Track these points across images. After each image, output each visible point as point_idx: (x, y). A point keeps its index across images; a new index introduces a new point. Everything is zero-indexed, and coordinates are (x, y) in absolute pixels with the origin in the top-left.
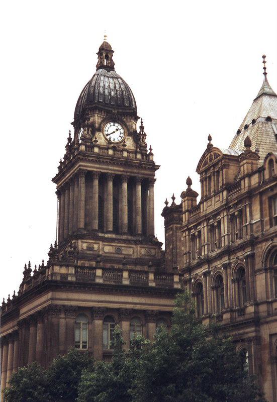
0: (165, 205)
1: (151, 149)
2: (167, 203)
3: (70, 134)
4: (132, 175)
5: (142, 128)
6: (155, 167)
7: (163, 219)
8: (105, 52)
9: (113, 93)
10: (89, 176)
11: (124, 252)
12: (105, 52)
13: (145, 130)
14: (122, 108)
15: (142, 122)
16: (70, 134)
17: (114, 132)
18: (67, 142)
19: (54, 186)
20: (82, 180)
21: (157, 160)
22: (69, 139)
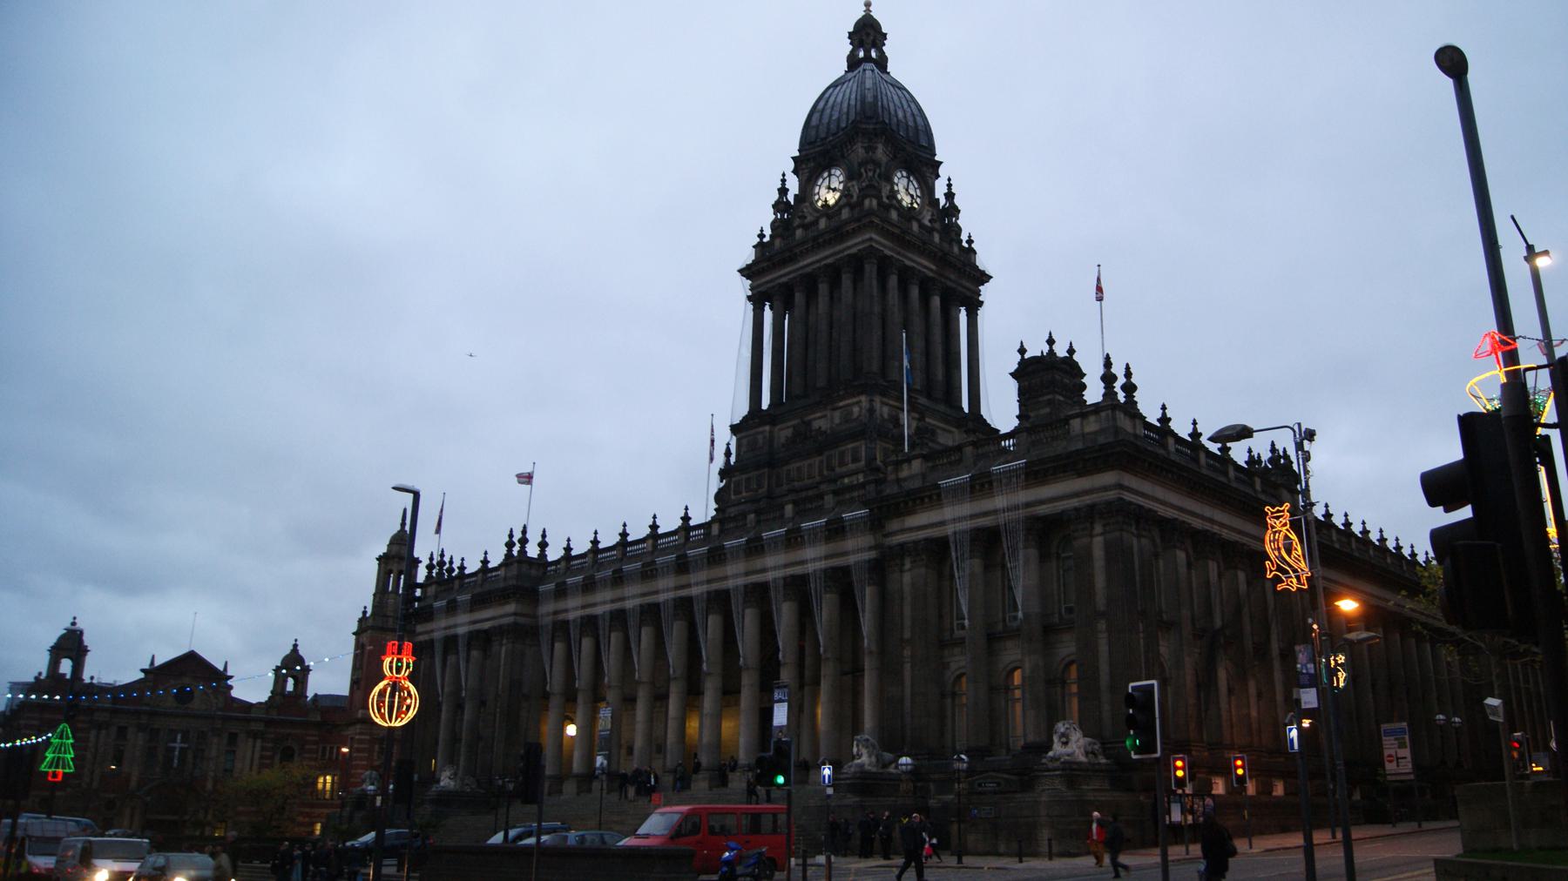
0: (1019, 357)
1: (970, 241)
2: (1022, 351)
3: (784, 181)
4: (949, 284)
5: (950, 196)
6: (984, 278)
7: (1013, 386)
8: (867, 35)
9: (900, 114)
10: (884, 265)
11: (941, 440)
12: (867, 35)
13: (957, 201)
14: (912, 147)
15: (949, 186)
16: (784, 181)
17: (905, 191)
18: (776, 196)
19: (743, 287)
20: (870, 269)
21: (983, 261)
22: (783, 191)
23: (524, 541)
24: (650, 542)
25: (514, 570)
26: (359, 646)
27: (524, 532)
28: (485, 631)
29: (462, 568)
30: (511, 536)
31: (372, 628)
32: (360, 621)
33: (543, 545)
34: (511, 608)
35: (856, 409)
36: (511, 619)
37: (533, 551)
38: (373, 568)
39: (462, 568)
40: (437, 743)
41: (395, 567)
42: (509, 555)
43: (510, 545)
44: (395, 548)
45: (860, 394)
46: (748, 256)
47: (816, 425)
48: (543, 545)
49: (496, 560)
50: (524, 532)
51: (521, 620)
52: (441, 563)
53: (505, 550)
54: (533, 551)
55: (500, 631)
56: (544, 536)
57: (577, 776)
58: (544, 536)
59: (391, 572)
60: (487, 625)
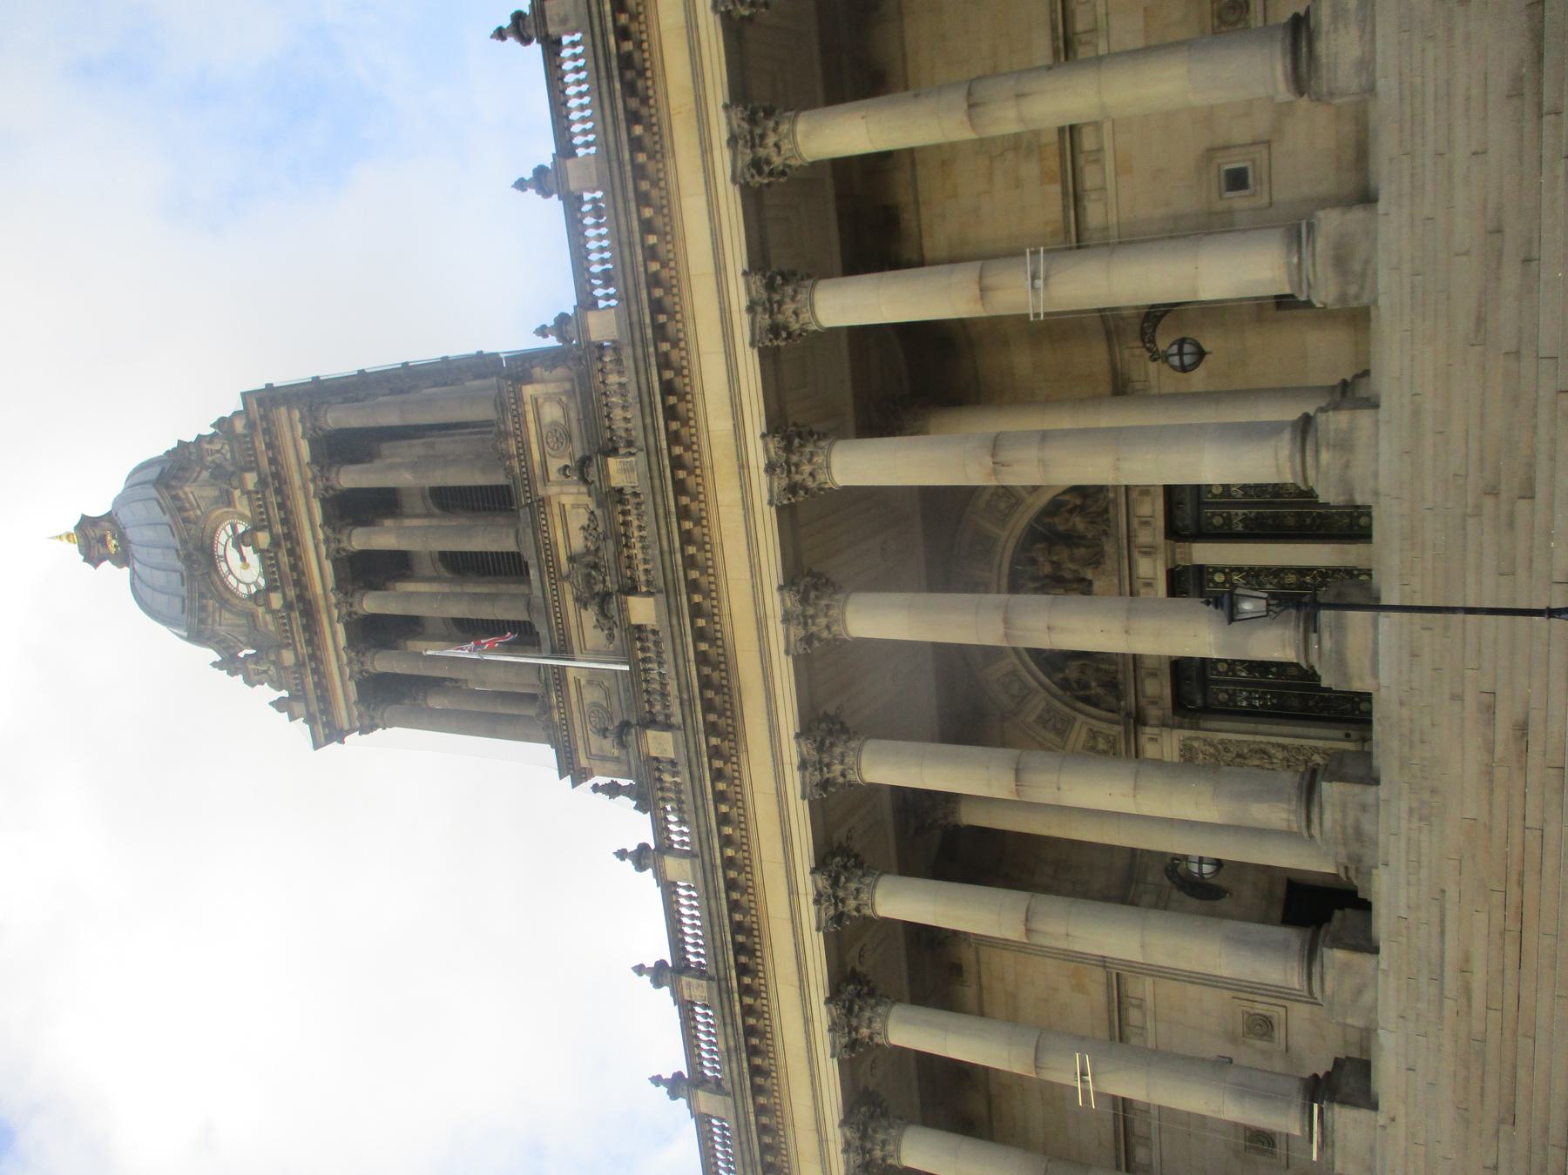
35: (552, 413)
45: (519, 399)
46: (300, 731)
47: (578, 543)
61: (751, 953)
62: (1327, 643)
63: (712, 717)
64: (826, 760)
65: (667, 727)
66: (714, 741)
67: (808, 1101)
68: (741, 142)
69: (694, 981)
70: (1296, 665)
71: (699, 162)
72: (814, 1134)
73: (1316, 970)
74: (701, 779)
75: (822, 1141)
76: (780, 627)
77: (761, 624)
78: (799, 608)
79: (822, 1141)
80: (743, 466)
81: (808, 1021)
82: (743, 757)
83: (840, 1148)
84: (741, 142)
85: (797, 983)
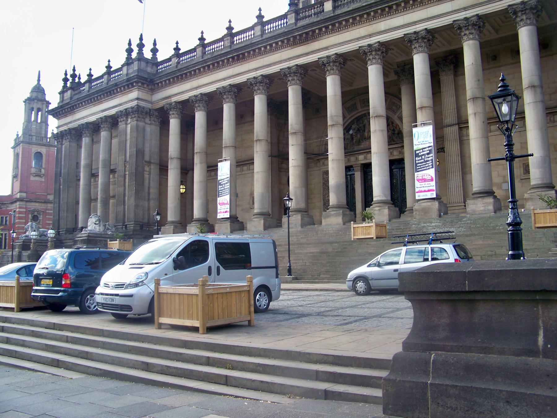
23: (141, 46)
24: (258, 28)
25: (135, 66)
26: (17, 156)
27: (141, 39)
28: (112, 117)
29: (90, 75)
30: (130, 44)
31: (22, 142)
32: (15, 140)
33: (155, 51)
34: (134, 94)
36: (135, 103)
37: (148, 54)
38: (21, 108)
39: (90, 75)
40: (77, 203)
41: (36, 106)
42: (129, 58)
43: (129, 51)
44: (35, 94)
48: (155, 51)
49: (118, 62)
50: (141, 39)
51: (142, 104)
52: (74, 76)
53: (125, 55)
54: (148, 54)
55: (126, 113)
56: (155, 44)
57: (198, 220)
58: (155, 44)
59: (32, 109)
60: (113, 112)
61: (238, 60)
62: (333, 213)
63: (298, 37)
64: (292, 75)
65: (297, 20)
66: (292, 39)
67: (205, 83)
68: (465, 22)
69: (229, 41)
70: (329, 205)
71: (462, 7)
72: (197, 86)
73: (258, 216)
74: (280, 37)
75: (196, 88)
76: (326, 55)
77: (326, 48)
78: (331, 60)
79: (196, 88)
80: (370, 36)
81: (224, 79)
82: (290, 48)
83: (195, 94)
84: (465, 22)
85: (234, 74)
